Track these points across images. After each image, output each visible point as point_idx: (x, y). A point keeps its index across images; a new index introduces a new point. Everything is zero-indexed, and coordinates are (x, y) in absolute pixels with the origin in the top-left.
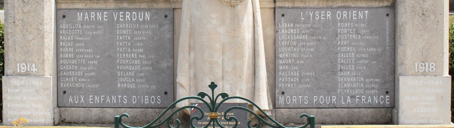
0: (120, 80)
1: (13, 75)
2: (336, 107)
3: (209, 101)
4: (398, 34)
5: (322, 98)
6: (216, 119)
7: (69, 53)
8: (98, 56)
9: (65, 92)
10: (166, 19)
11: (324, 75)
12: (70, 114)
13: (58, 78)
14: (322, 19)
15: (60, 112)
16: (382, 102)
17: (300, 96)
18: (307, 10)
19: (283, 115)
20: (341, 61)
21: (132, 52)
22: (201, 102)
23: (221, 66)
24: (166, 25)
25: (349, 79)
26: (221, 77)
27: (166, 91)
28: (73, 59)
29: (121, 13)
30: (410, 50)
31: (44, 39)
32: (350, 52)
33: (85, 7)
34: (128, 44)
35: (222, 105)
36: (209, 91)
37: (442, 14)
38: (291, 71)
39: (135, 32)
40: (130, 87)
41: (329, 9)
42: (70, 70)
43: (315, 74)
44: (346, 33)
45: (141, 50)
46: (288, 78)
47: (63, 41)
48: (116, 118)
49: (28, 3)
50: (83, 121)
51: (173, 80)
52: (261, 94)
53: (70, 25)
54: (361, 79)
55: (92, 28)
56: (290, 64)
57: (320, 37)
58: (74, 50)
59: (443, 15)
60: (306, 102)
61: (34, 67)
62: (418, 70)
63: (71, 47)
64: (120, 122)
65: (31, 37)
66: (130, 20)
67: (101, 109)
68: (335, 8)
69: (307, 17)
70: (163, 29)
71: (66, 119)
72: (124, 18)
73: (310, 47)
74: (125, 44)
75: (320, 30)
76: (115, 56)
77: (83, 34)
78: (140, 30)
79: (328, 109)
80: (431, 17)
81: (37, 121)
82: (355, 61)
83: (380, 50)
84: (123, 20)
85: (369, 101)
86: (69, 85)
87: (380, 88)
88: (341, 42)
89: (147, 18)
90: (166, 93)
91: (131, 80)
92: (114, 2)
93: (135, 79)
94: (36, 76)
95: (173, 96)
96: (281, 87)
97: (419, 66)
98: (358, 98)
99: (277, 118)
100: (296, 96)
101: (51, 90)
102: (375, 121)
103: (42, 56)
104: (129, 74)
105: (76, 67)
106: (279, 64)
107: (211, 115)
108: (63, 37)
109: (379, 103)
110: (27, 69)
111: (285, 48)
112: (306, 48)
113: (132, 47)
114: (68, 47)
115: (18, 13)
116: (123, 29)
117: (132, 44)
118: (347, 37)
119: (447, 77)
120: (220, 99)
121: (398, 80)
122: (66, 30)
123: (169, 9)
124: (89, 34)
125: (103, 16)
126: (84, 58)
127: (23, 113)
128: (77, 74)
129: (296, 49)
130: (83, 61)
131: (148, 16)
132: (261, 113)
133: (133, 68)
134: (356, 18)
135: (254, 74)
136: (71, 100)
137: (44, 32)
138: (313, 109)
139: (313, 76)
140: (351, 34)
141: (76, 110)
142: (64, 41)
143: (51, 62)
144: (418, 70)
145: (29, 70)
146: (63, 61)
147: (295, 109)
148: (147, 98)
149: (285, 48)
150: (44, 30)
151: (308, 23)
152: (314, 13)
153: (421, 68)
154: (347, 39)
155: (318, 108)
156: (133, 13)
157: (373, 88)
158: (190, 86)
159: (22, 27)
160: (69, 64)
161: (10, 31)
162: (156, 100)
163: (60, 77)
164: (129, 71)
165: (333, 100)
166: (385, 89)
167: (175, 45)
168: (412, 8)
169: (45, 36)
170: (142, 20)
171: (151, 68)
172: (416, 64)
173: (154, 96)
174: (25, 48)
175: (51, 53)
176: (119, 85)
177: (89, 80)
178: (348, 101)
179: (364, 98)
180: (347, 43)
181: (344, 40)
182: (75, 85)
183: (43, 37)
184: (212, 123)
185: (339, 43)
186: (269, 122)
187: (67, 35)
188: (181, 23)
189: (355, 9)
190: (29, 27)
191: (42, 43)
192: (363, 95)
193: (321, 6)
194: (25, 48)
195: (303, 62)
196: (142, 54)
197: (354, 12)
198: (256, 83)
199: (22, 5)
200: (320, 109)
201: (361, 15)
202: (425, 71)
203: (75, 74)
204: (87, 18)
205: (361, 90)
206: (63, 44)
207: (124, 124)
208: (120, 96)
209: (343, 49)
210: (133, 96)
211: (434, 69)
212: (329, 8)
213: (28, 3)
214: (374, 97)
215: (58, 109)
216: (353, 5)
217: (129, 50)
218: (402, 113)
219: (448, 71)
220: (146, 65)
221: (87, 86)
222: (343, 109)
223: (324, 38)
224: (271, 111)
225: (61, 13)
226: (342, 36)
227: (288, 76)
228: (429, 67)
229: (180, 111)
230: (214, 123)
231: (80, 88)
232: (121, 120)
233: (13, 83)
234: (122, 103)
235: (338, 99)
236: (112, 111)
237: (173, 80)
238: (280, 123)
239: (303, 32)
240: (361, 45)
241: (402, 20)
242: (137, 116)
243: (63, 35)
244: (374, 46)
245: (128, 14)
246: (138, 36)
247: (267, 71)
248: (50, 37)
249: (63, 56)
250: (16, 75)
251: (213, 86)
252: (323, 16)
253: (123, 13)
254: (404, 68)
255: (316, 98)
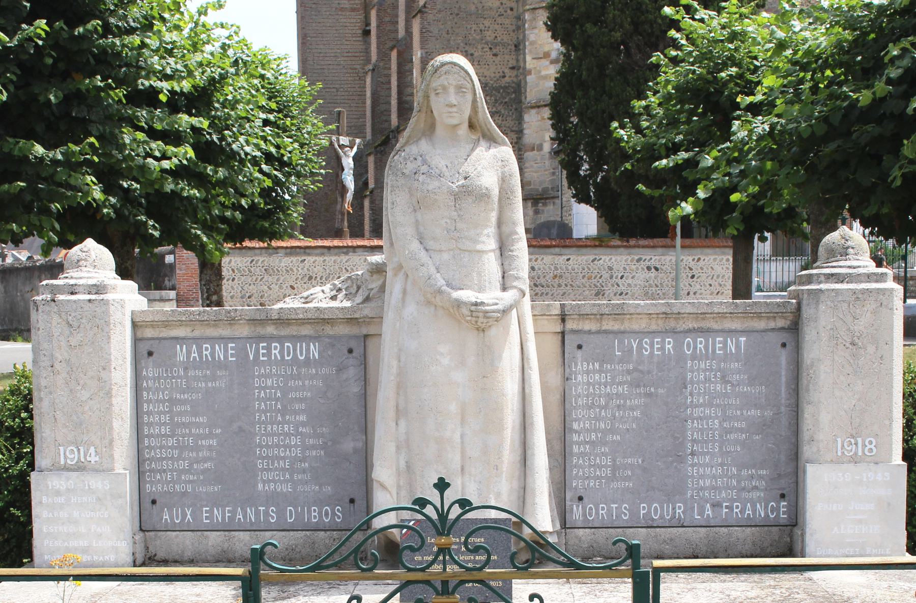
0: (262, 477)
1: (51, 470)
2: (685, 524)
3: (434, 516)
4: (804, 382)
5: (656, 508)
6: (449, 549)
7: (161, 424)
8: (219, 431)
9: (154, 502)
10: (350, 355)
11: (659, 463)
12: (165, 543)
13: (140, 474)
14: (656, 353)
15: (145, 541)
16: (773, 514)
17: (614, 503)
18: (627, 335)
19: (580, 541)
20: (692, 435)
21: (284, 422)
22: (420, 517)
23: (459, 446)
24: (352, 368)
25: (708, 470)
26: (460, 469)
27: (352, 496)
28: (169, 436)
29: (261, 345)
30: (828, 413)
31: (111, 397)
32: (711, 417)
33: (190, 335)
34: (276, 406)
35: (460, 523)
36: (433, 496)
37: (889, 343)
38: (596, 455)
39: (291, 383)
40: (282, 489)
41: (669, 334)
42: (164, 459)
43: (643, 461)
44: (702, 382)
45: (302, 418)
46: (589, 469)
47: (149, 402)
48: (254, 550)
49: (79, 327)
50: (191, 558)
51: (366, 476)
52: (537, 500)
53: (162, 370)
54: (731, 470)
55: (206, 376)
56: (594, 442)
57: (652, 390)
58: (172, 419)
59: (892, 345)
60: (625, 515)
61: (93, 454)
62: (843, 453)
63: (165, 413)
64: (262, 558)
65: (85, 395)
66: (279, 358)
67: (226, 533)
68: (681, 332)
69: (626, 349)
70: (345, 376)
71: (158, 554)
72: (269, 354)
73: (632, 409)
74: (271, 405)
75: (652, 376)
76: (252, 430)
77: (188, 387)
78: (300, 379)
79: (669, 529)
80: (868, 348)
81: (101, 559)
82: (721, 436)
83: (768, 413)
84: (266, 359)
85: (747, 512)
86: (163, 488)
87: (768, 488)
88: (693, 398)
89: (313, 354)
90: (352, 501)
91: (284, 476)
92: (249, 324)
93: (291, 475)
94: (97, 471)
95: (365, 505)
96: (576, 488)
97: (845, 444)
98: (727, 507)
99: (569, 547)
100: (606, 504)
101: (126, 496)
102: (758, 551)
103: (109, 431)
104: (279, 465)
105: (176, 453)
106: (573, 443)
107: (438, 542)
108: (148, 393)
109: (767, 515)
110: (79, 458)
111: (583, 410)
112: (624, 411)
113: (284, 412)
114: (160, 413)
115: (60, 348)
116: (267, 376)
117: (284, 407)
118: (705, 389)
119: (899, 465)
120: (456, 511)
121: (804, 472)
122: (155, 381)
123: (356, 337)
124: (201, 388)
125: (226, 351)
126: (190, 435)
127: (73, 543)
128: (178, 466)
129: (605, 412)
130: (188, 440)
131: (314, 350)
132: (538, 538)
133: (288, 453)
134: (721, 352)
135: (522, 461)
136: (167, 517)
137: (111, 384)
138: (640, 529)
139: (639, 465)
140: (713, 383)
141: (177, 537)
142: (151, 402)
143: (126, 442)
144: (843, 453)
145: (83, 460)
146: (149, 442)
147: (605, 530)
148: (315, 511)
149: (583, 410)
150: (110, 380)
151: (628, 362)
152: (640, 343)
153: (849, 448)
154: (705, 392)
155: (648, 527)
156: (286, 344)
157: (756, 488)
158: (399, 487)
159: (68, 376)
160: (161, 447)
161: (43, 383)
162: (334, 514)
163: (144, 473)
164: (279, 458)
165: (677, 511)
166: (779, 489)
167: (368, 406)
168: (831, 332)
169: (114, 392)
170: (303, 358)
171: (322, 453)
172: (839, 440)
173: (328, 506)
174: (74, 417)
175: (125, 426)
176: (260, 486)
177: (202, 477)
178: (707, 513)
179: (737, 507)
180: (704, 401)
181: (699, 394)
182: (174, 487)
183: (109, 394)
184: (441, 558)
185: (689, 400)
186: (553, 555)
187: (157, 390)
188: (381, 364)
189: (720, 333)
190: (82, 375)
191: (108, 406)
192: (733, 500)
193: (654, 327)
194: (74, 417)
195: (619, 437)
196: (303, 424)
197: (718, 339)
198: (527, 480)
199: (67, 332)
200: (652, 529)
201: (731, 346)
202: (856, 454)
203: (173, 465)
204: (196, 355)
205: (732, 492)
206: (148, 407)
207: (269, 561)
208: (262, 508)
209: (698, 412)
210: (289, 508)
211: (874, 450)
212: (670, 332)
213: (79, 327)
214: (758, 506)
215: (141, 534)
216: (715, 326)
217: (280, 418)
218: (811, 535)
219: (901, 453)
220: (313, 447)
221: (198, 489)
222: (697, 528)
223: (660, 391)
224: (558, 533)
225: (144, 348)
226: (696, 387)
227: (590, 466)
228: (864, 446)
229: (380, 535)
230: (444, 558)
231: (185, 494)
232: (264, 554)
233: (53, 486)
234: (266, 520)
235: (688, 510)
236: (248, 538)
237: (367, 476)
238: (574, 557)
239: (619, 379)
240: (732, 404)
241: (811, 356)
242: (296, 546)
243: (148, 389)
244: (756, 406)
245: (276, 348)
246: (296, 389)
247: (549, 456)
248: (123, 394)
249: (149, 430)
250: (58, 470)
251: (442, 485)
252: (658, 348)
253: (265, 344)
254: (815, 449)
255: (644, 508)
